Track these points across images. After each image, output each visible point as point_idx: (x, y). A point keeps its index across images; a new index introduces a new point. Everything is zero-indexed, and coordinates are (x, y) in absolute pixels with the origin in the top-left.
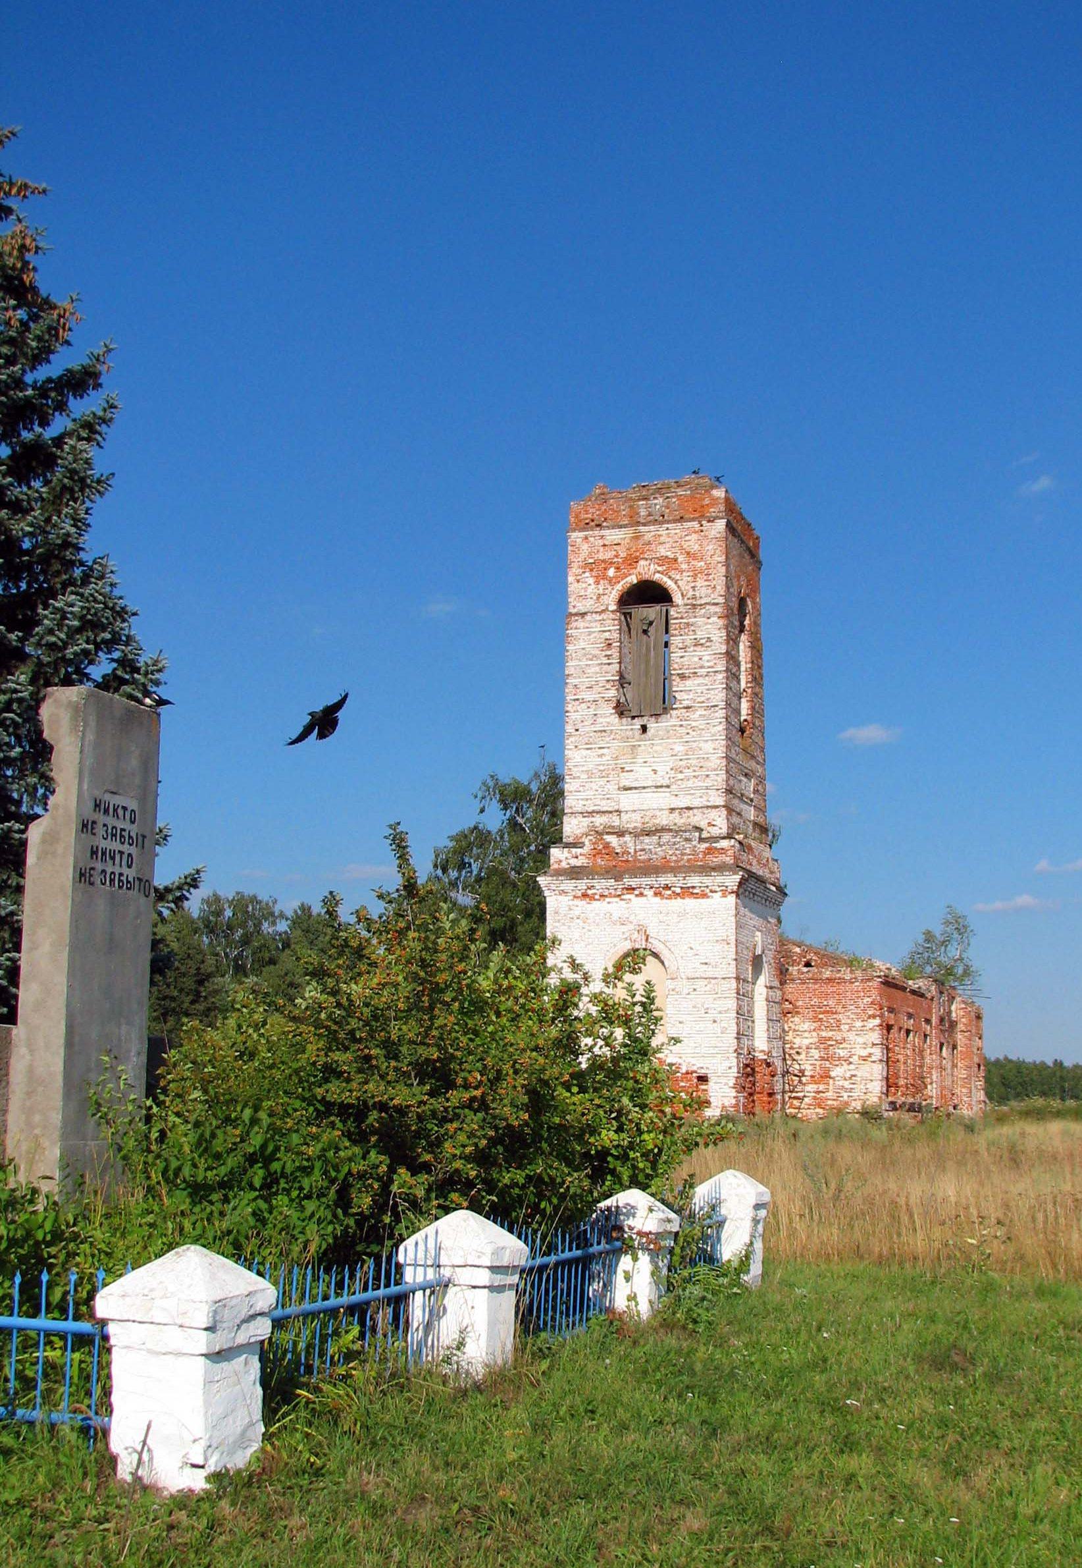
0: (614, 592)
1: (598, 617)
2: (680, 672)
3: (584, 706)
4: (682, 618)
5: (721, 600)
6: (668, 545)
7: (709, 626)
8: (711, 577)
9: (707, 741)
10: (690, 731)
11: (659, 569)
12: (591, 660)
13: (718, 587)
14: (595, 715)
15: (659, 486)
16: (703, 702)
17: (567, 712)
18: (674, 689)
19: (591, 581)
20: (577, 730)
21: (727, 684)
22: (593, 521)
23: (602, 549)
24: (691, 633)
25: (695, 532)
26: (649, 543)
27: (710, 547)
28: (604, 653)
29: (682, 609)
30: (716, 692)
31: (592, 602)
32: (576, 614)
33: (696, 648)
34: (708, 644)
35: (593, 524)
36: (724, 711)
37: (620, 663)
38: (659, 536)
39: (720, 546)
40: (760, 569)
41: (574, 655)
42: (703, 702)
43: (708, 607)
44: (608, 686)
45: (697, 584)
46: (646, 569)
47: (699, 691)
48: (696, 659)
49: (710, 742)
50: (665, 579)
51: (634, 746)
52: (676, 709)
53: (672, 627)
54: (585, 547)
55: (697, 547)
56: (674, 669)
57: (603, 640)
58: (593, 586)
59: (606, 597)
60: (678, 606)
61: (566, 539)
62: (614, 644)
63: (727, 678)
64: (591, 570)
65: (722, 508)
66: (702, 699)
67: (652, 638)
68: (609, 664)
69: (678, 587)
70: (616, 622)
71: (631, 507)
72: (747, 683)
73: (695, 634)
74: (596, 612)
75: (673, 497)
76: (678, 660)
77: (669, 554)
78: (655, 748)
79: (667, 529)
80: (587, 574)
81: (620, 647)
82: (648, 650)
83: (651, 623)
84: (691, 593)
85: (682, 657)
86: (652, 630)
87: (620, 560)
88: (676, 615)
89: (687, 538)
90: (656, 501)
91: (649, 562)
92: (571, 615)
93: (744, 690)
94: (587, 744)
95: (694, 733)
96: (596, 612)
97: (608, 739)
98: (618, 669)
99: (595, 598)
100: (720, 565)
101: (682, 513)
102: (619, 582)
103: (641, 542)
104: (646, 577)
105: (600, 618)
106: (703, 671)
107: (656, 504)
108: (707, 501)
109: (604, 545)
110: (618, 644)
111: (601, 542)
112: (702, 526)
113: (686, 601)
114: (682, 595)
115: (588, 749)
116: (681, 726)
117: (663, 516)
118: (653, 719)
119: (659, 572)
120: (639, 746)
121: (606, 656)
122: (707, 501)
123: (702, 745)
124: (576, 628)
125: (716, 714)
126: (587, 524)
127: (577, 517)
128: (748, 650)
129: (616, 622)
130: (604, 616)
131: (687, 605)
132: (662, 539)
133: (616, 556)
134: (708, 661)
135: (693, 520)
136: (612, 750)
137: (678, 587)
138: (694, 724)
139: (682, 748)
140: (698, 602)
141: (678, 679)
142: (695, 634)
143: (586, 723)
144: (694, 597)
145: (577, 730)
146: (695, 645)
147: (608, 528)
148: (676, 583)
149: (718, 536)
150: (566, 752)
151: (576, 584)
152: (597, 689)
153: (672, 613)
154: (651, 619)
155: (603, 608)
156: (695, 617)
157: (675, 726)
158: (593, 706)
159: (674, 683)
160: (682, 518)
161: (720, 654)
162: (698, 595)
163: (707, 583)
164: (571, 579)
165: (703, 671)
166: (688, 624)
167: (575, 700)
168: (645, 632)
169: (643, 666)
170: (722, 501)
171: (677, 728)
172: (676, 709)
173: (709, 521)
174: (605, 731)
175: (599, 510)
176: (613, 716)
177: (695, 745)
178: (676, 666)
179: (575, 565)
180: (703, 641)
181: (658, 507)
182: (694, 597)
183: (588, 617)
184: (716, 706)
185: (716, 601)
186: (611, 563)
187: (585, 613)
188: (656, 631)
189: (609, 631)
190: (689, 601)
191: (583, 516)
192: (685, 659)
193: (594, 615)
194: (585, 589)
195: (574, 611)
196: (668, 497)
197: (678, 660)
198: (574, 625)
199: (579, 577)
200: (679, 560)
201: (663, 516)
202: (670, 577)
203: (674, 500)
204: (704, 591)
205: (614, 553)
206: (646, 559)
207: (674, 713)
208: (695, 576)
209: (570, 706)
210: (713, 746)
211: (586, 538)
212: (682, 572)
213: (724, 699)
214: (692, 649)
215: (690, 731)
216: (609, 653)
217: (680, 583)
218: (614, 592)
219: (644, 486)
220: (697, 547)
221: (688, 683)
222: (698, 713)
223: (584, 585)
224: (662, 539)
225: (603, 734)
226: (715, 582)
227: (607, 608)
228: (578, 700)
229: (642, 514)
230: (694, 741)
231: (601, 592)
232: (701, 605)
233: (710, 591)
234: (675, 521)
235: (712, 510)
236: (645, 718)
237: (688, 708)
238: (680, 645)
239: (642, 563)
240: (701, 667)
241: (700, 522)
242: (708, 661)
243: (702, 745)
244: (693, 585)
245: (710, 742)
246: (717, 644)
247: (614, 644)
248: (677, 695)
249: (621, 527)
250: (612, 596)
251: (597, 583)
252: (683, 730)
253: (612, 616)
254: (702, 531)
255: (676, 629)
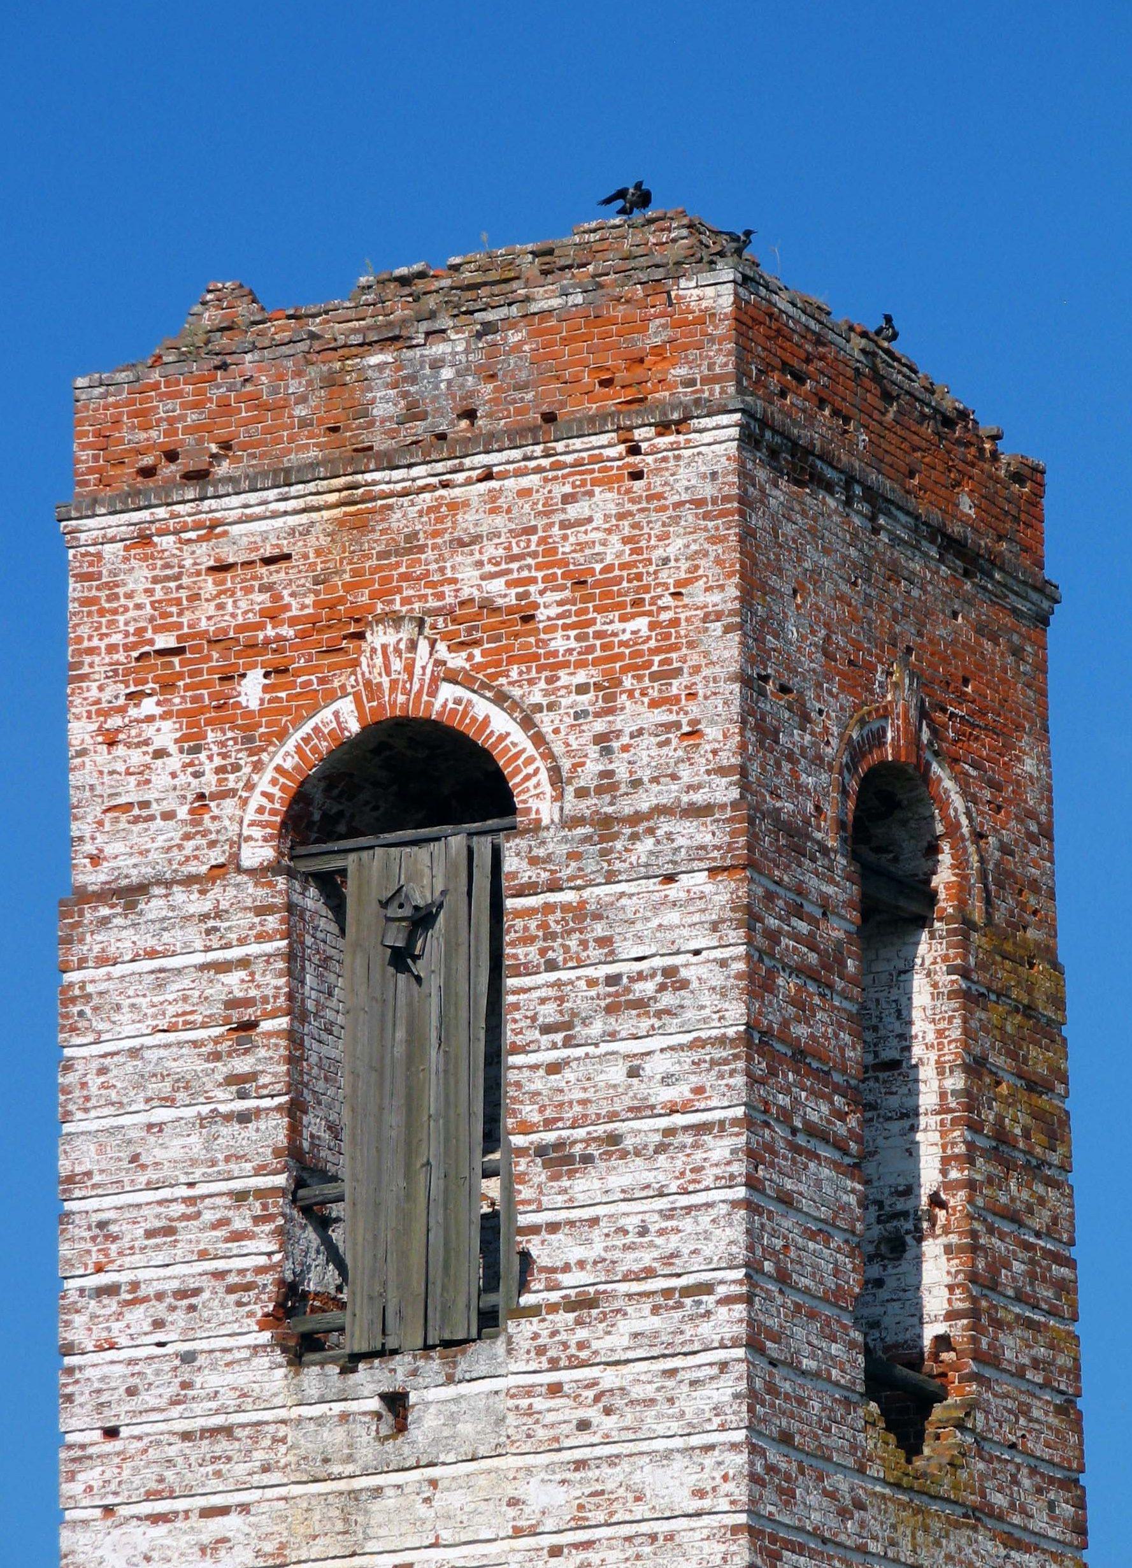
0: (264, 782)
1: (194, 903)
2: (550, 1137)
3: (139, 1317)
4: (554, 887)
5: (724, 791)
6: (491, 550)
7: (672, 917)
8: (676, 687)
9: (668, 1454)
10: (593, 1413)
11: (457, 661)
12: (169, 1101)
13: (712, 733)
14: (188, 1358)
15: (467, 276)
16: (649, 1273)
17: (69, 1349)
18: (523, 1220)
19: (166, 734)
20: (111, 1433)
21: (752, 1183)
22: (172, 456)
23: (209, 586)
24: (595, 953)
25: (606, 482)
26: (412, 545)
27: (675, 547)
28: (222, 1069)
29: (555, 845)
30: (705, 1219)
31: (171, 832)
32: (105, 895)
33: (613, 1023)
34: (667, 999)
35: (170, 470)
36: (740, 1310)
37: (295, 1110)
38: (454, 506)
39: (714, 540)
40: (1043, 620)
41: (94, 1082)
42: (649, 1273)
43: (665, 826)
44: (240, 1223)
45: (619, 721)
46: (397, 665)
47: (632, 1223)
48: (617, 1073)
49: (679, 1462)
50: (482, 707)
51: (354, 1495)
52: (533, 1311)
53: (514, 929)
54: (138, 578)
55: (614, 550)
56: (526, 1128)
57: (217, 1009)
58: (175, 762)
59: (229, 806)
60: (536, 827)
61: (62, 544)
62: (266, 1025)
63: (753, 1155)
64: (167, 686)
65: (723, 359)
66: (647, 1258)
67: (434, 983)
68: (244, 1118)
69: (539, 740)
70: (273, 922)
71: (332, 382)
72: (945, 1161)
73: (611, 958)
74: (190, 880)
75: (510, 323)
76: (539, 1083)
77: (496, 586)
78: (441, 1499)
79: (488, 476)
80: (149, 706)
81: (293, 1037)
82: (415, 1039)
83: (423, 920)
84: (593, 766)
85: (554, 1068)
86: (433, 944)
87: (287, 631)
88: (528, 874)
89: (573, 511)
90: (439, 349)
91: (408, 631)
92: (84, 897)
93: (936, 1201)
94: (152, 1496)
95: (610, 1422)
96: (190, 880)
97: (240, 1469)
98: (281, 1138)
99: (183, 813)
100: (717, 628)
101: (553, 395)
102: (283, 735)
103: (375, 542)
104: (398, 703)
105: (207, 906)
106: (649, 1128)
107: (437, 365)
108: (656, 334)
109: (222, 568)
110: (283, 1022)
111: (205, 556)
112: (634, 450)
113: (572, 806)
114: (556, 776)
115: (156, 1519)
116: (555, 1389)
117: (470, 415)
118: (434, 1366)
119: (452, 678)
120: (377, 1492)
121: (233, 1079)
122: (656, 334)
123: (647, 1475)
124: (104, 960)
125: (705, 1329)
126: (148, 472)
127: (104, 440)
128: (949, 1006)
129: (273, 922)
130: (221, 895)
131: (577, 821)
132: (467, 521)
133: (272, 615)
134: (668, 1080)
135: (594, 424)
136: (261, 1520)
137: (539, 740)
138: (609, 1378)
139: (558, 1496)
140: (626, 807)
141: (538, 1173)
142: (611, 958)
143: (149, 1399)
144: (607, 784)
145: (111, 1433)
146: (610, 1010)
147: (236, 486)
148: (527, 723)
149: (708, 490)
150: (67, 1539)
151: (102, 756)
152: (191, 1236)
153: (510, 864)
154: (421, 897)
155: (217, 856)
156: (611, 878)
157: (529, 1391)
158: (179, 1318)
159: (525, 1192)
160: (549, 418)
161: (722, 1041)
162: (622, 773)
163: (661, 716)
164: (80, 731)
165: (649, 1128)
166: (579, 913)
167: (101, 1292)
168: (401, 959)
169: (394, 1119)
170: (723, 328)
171: (539, 1404)
172: (533, 1311)
173: (664, 428)
174: (227, 1431)
175: (196, 405)
176: (263, 1361)
177: (611, 1478)
178: (530, 1113)
179: (99, 665)
180: (647, 988)
181: (447, 373)
182: (607, 784)
183: (154, 907)
184: (707, 1288)
185: (699, 797)
186: (251, 647)
187: (142, 889)
188: (451, 950)
189: (244, 963)
190: (585, 807)
191: (131, 436)
192: (568, 1074)
193: (179, 895)
194: (143, 775)
195: (91, 878)
196: (488, 328)
197: (539, 1083)
198: (93, 943)
199: (115, 722)
200: (542, 614)
201: (470, 415)
202: (500, 699)
203: (514, 337)
204: (647, 751)
205: (261, 599)
206: (397, 620)
207: (522, 1330)
208: (608, 689)
209: (79, 1320)
210: (691, 1480)
211: (144, 539)
212: (554, 666)
213: (740, 1252)
214: (597, 1028)
215: (593, 1413)
216: (242, 1065)
217: (546, 722)
218: (264, 782)
219: (404, 281)
220: (614, 550)
221: (584, 1186)
222: (625, 1327)
223: (136, 757)
224: (467, 521)
225: (223, 1445)
226: (694, 709)
227: (235, 857)
228: (112, 1290)
229: (380, 410)
230: (613, 1461)
231: (209, 782)
232: (636, 818)
233: (675, 750)
234: (516, 437)
235: (681, 371)
236: (401, 1364)
237: (583, 1303)
238: (549, 1013)
239: (380, 637)
240: (641, 1110)
241: (625, 435)
242: (668, 1080)
243: (647, 1475)
244: (600, 726)
245: (679, 1462)
246: (706, 999)
247: (266, 1025)
248: (534, 1246)
249: (285, 478)
250: (256, 800)
251: (192, 743)
252: (564, 1411)
253: (254, 893)
254: (637, 475)
255: (529, 940)
